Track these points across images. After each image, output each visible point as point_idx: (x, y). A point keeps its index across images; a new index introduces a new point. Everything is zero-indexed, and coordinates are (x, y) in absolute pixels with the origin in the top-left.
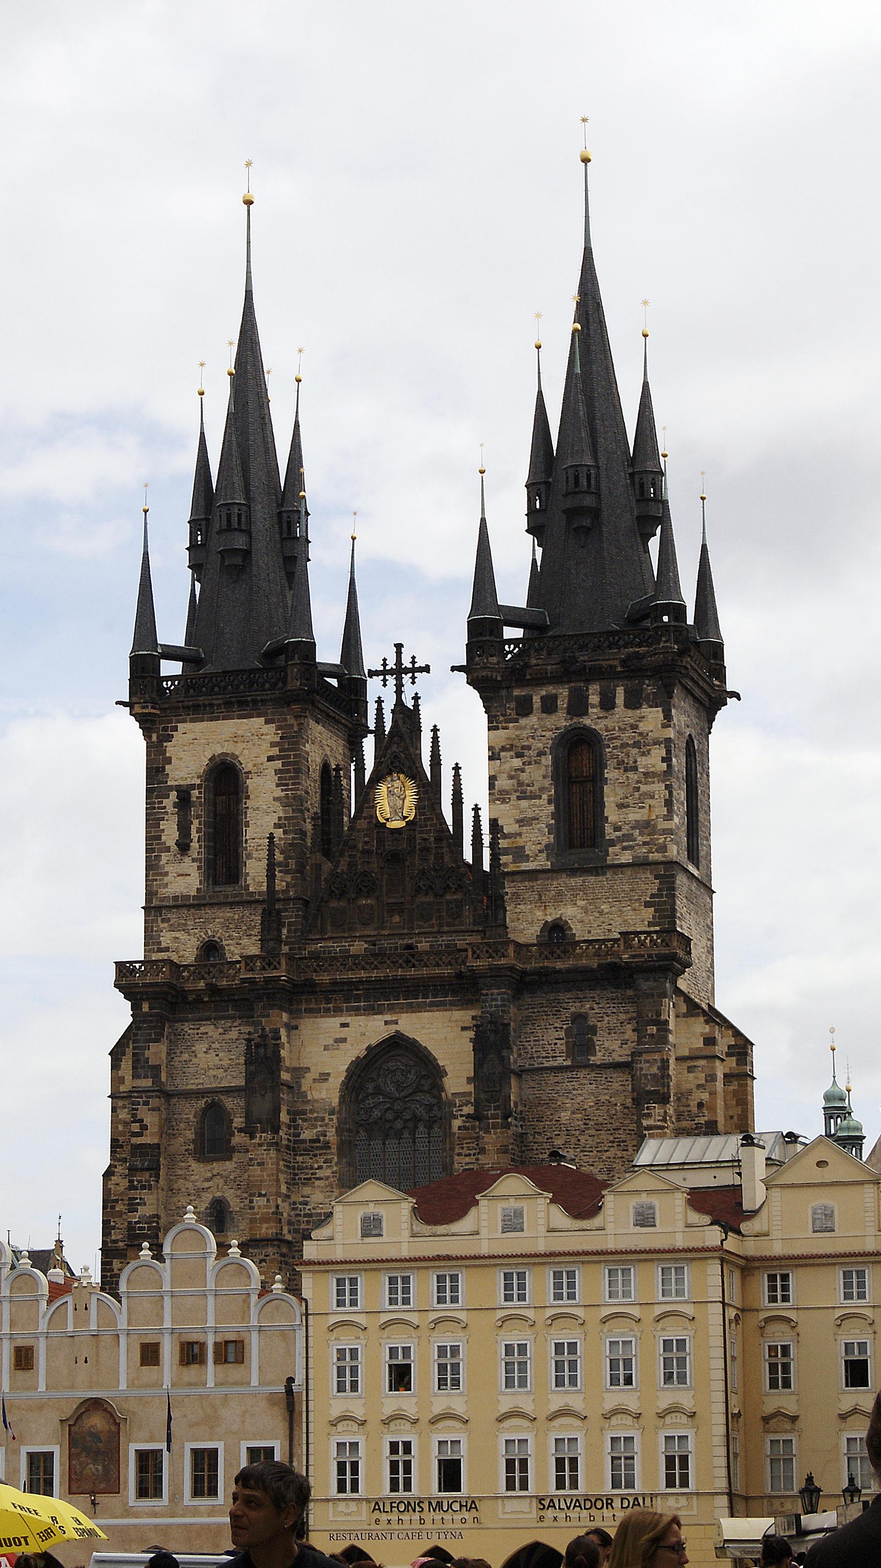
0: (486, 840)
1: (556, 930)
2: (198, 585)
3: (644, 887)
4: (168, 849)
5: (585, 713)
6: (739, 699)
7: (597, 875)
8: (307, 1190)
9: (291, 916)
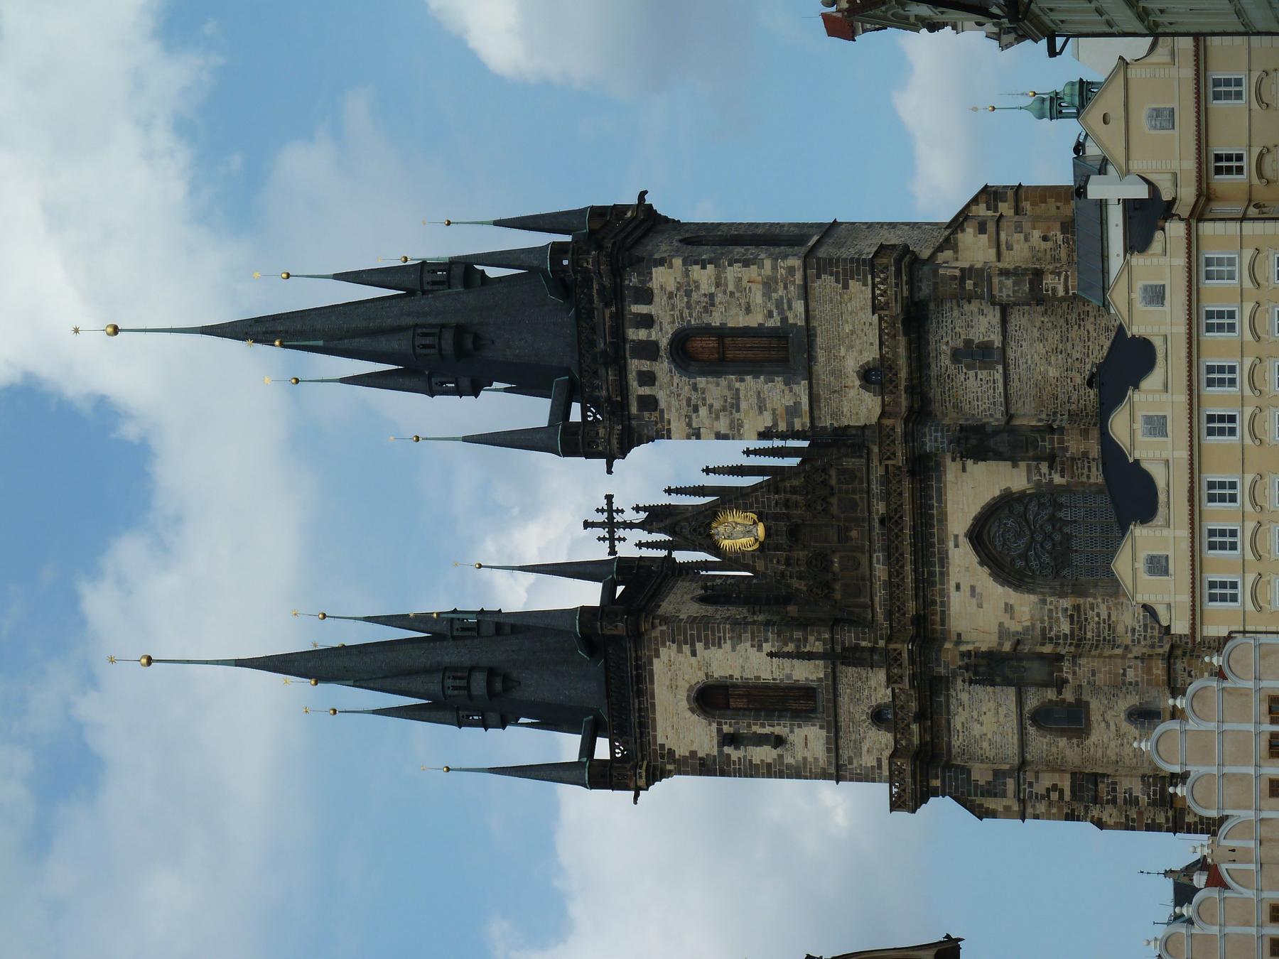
0: (778, 443)
1: (868, 376)
2: (522, 720)
3: (828, 290)
4: (781, 757)
5: (655, 345)
6: (646, 192)
7: (815, 335)
8: (1120, 629)
9: (849, 637)
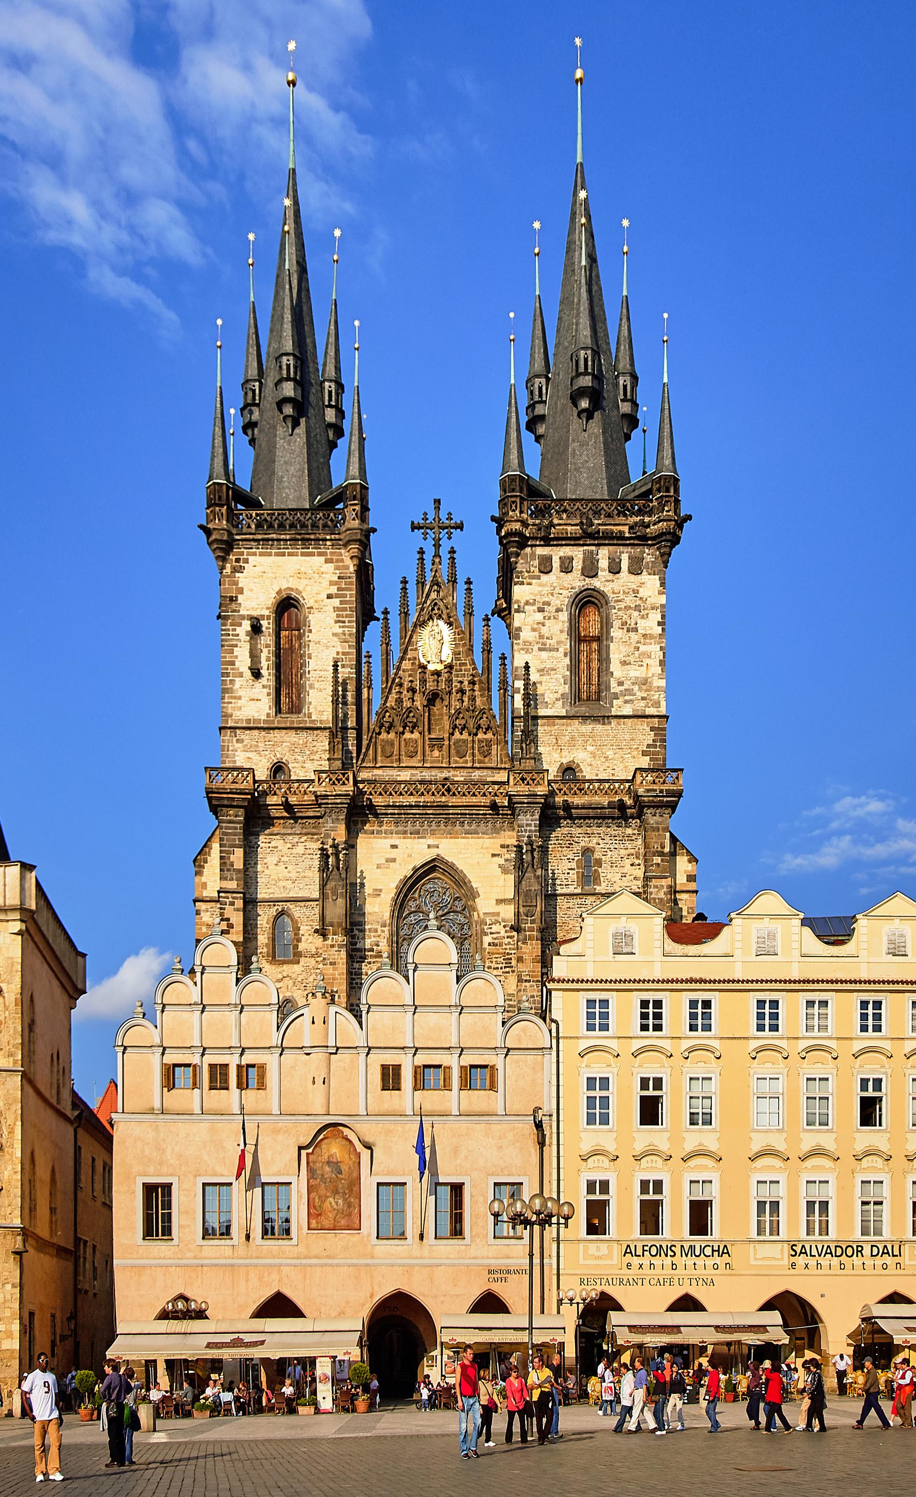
5: (596, 575)
